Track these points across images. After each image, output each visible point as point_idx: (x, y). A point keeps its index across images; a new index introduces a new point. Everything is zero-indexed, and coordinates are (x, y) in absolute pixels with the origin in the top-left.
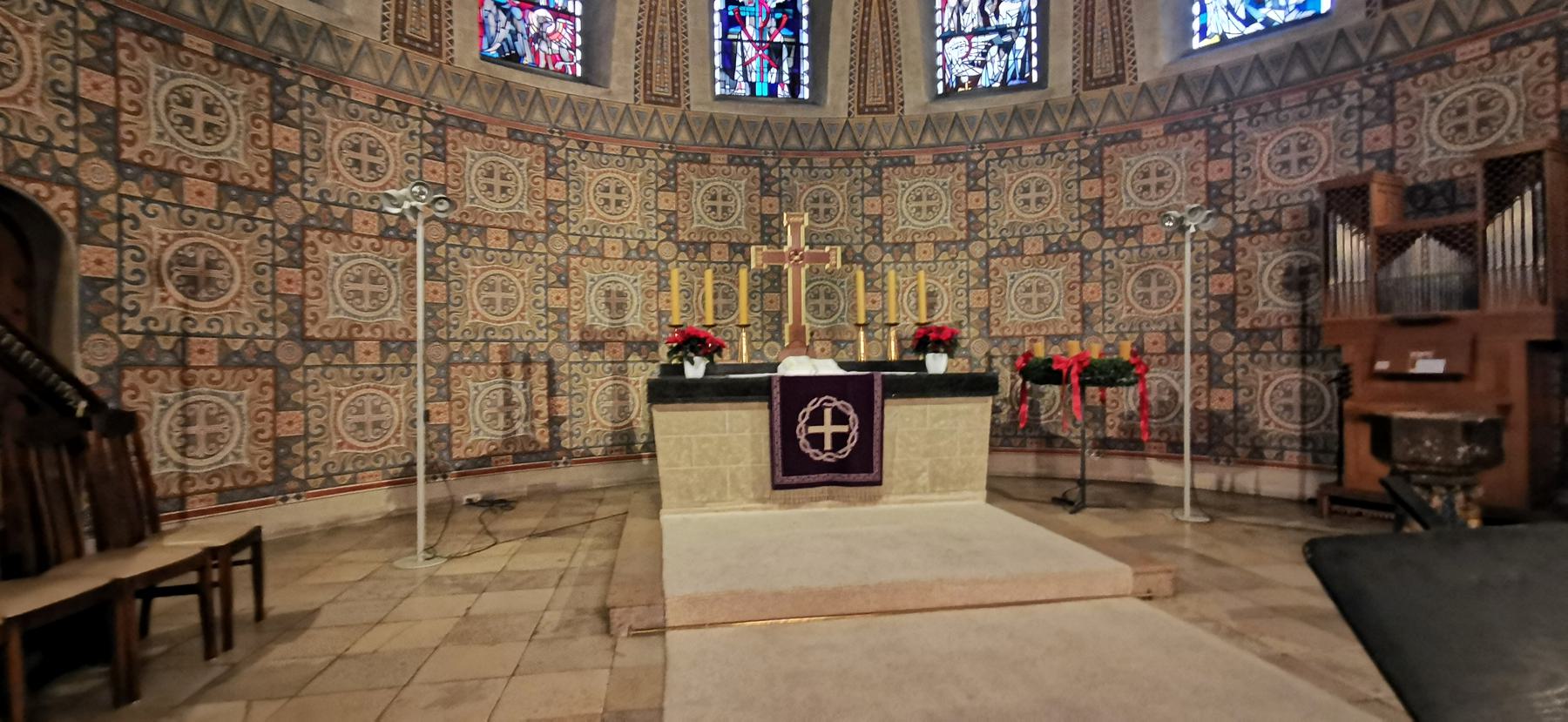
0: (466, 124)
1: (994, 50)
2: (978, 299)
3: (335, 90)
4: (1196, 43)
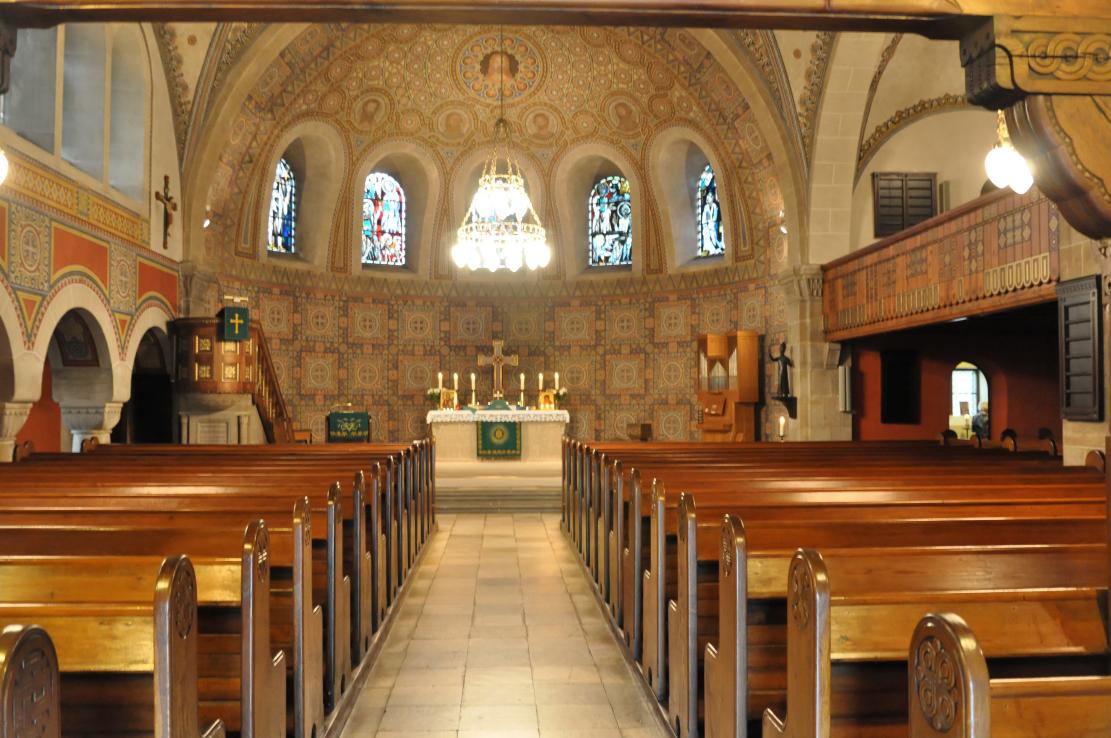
0: (356, 299)
1: (617, 243)
2: (600, 375)
3: (312, 295)
4: (700, 253)
